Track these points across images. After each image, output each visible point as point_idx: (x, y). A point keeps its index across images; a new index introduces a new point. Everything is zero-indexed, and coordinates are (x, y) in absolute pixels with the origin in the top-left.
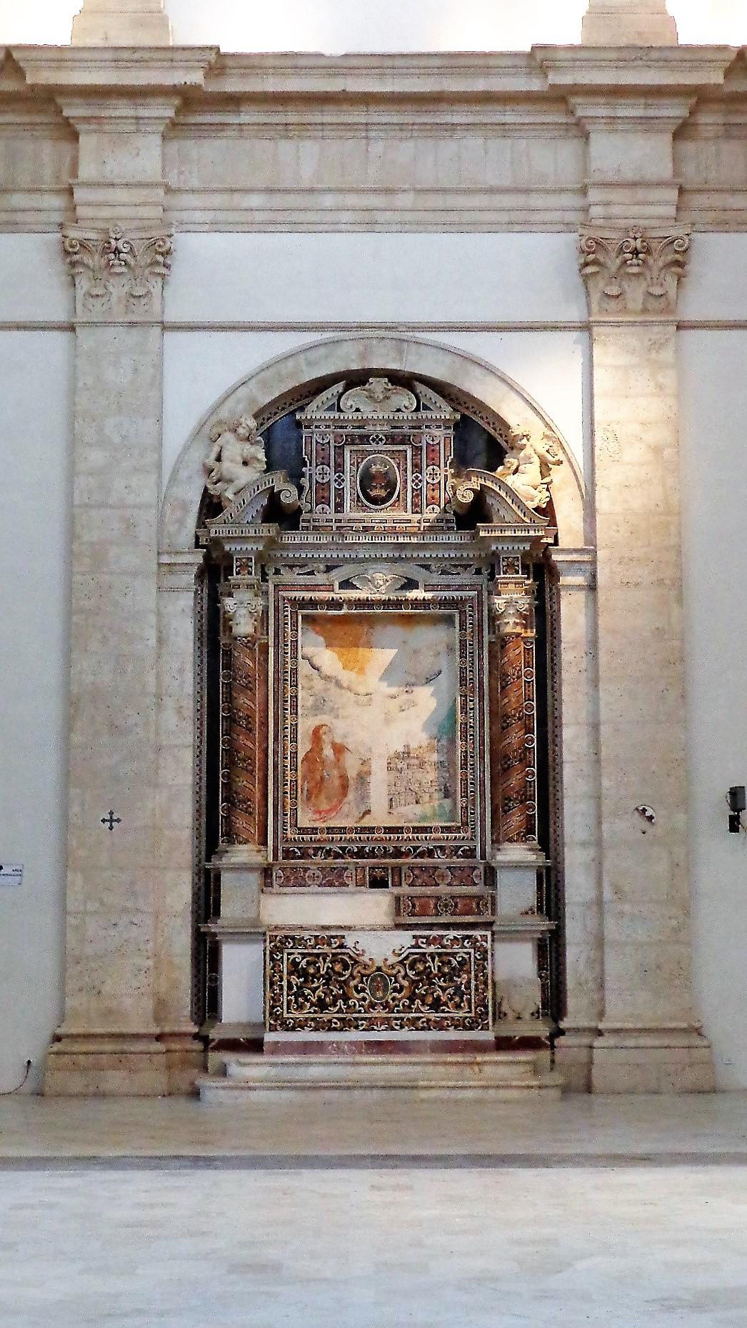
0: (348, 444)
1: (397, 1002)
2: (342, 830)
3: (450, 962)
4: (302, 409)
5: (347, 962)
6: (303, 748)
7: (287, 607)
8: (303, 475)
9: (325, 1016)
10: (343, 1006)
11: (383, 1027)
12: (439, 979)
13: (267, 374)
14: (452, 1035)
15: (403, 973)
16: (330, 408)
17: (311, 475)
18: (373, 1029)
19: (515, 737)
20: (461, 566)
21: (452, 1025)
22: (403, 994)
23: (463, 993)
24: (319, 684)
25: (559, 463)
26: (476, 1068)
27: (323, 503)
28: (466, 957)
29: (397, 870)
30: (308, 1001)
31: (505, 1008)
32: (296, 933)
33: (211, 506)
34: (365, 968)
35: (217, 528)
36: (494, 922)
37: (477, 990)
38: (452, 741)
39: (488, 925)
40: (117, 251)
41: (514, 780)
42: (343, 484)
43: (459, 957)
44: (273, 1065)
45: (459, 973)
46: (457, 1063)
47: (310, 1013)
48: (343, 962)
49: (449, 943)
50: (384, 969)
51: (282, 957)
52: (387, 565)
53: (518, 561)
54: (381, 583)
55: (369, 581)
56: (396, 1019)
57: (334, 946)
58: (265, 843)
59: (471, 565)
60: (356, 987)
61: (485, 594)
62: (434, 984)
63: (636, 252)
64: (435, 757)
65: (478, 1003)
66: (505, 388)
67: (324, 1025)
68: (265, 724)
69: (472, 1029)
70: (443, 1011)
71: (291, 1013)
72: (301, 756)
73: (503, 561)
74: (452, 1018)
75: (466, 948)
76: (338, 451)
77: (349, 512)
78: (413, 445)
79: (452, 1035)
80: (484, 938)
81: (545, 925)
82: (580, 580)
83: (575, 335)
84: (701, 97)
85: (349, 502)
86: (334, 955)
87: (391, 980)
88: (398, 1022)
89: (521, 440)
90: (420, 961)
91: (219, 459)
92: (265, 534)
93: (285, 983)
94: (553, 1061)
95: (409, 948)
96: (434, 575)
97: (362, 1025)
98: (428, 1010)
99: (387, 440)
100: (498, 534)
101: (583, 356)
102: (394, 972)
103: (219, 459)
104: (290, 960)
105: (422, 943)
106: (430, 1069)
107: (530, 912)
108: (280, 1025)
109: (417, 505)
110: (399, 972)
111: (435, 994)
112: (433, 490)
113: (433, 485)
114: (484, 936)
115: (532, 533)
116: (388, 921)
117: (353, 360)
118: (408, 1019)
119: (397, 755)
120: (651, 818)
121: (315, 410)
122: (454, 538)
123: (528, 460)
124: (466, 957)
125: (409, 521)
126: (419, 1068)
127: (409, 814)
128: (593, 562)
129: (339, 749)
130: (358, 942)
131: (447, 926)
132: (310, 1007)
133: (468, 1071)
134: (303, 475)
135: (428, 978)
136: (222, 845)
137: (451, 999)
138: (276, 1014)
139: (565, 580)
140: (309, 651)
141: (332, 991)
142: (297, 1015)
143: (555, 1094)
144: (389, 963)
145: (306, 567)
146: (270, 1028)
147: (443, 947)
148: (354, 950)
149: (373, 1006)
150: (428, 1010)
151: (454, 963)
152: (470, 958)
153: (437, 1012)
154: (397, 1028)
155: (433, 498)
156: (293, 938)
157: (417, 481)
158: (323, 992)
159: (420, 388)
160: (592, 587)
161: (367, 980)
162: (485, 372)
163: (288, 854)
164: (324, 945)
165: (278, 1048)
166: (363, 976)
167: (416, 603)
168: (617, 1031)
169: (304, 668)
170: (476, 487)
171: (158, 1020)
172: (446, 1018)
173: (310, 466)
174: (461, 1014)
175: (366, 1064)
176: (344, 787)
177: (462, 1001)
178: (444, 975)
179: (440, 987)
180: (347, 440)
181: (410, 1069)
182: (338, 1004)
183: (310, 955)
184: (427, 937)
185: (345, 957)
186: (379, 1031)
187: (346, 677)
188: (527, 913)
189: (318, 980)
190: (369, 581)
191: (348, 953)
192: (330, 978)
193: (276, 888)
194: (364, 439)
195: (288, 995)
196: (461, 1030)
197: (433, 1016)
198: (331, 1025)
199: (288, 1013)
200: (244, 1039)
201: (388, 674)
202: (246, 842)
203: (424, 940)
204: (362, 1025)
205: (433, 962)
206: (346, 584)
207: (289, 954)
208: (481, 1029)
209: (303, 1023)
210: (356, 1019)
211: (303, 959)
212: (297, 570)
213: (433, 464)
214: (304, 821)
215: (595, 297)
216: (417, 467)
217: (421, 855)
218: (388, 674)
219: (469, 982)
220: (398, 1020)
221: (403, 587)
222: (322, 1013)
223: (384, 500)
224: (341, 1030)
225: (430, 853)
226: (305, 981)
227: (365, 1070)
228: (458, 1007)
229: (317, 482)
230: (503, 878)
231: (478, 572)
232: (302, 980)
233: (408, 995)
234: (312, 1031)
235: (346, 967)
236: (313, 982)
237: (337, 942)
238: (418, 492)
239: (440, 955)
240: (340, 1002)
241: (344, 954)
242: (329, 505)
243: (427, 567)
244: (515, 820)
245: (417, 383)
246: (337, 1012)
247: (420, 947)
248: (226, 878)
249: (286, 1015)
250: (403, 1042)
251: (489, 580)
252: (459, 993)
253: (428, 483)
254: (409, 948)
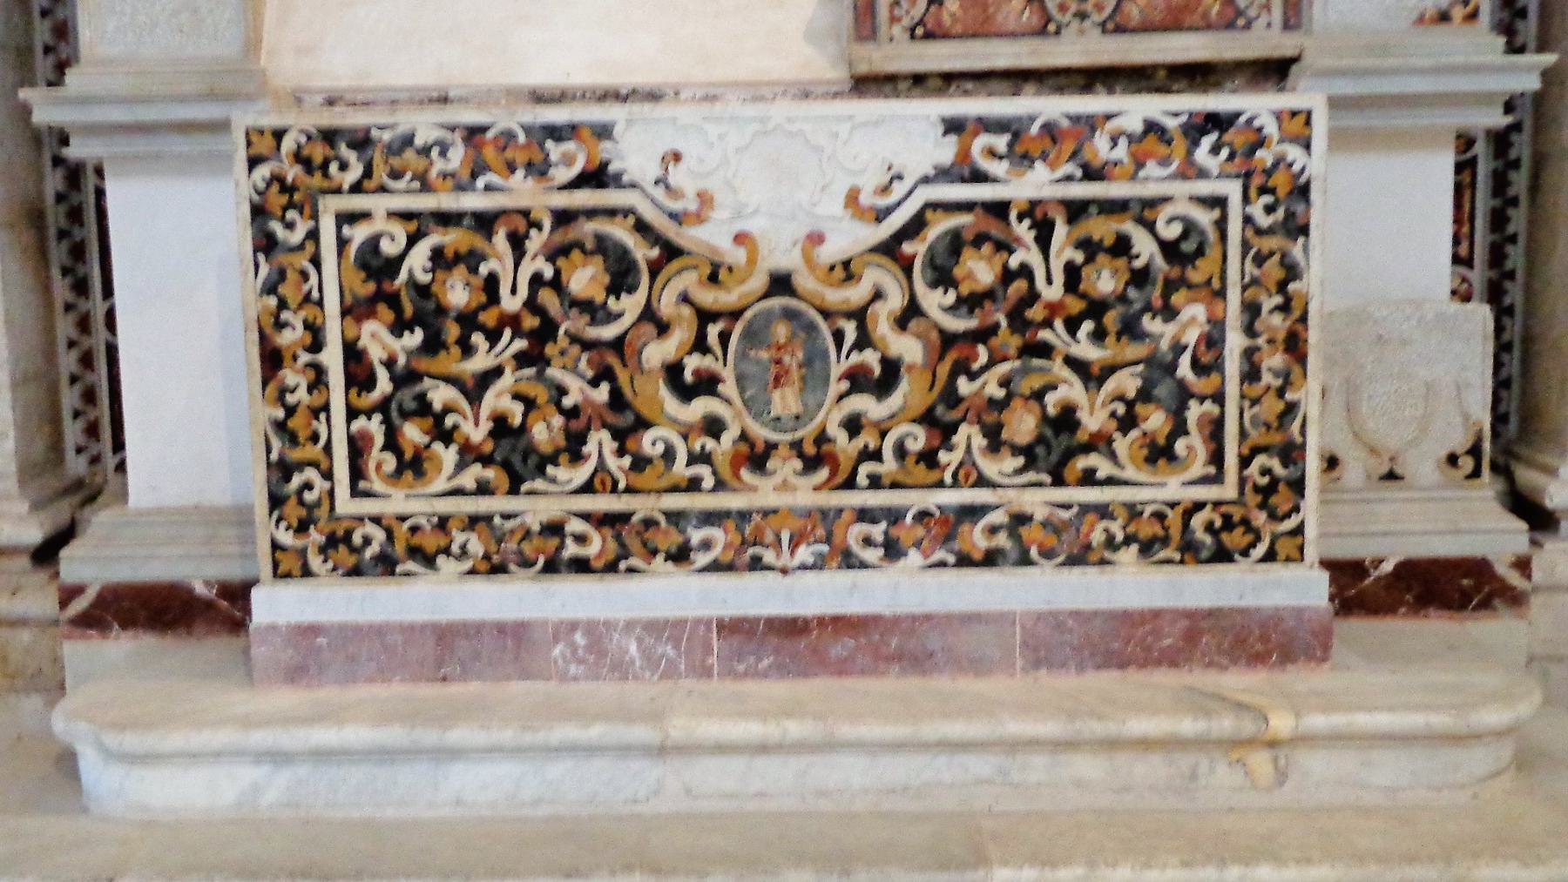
1: (867, 439)
3: (1122, 246)
9: (535, 509)
10: (613, 463)
11: (804, 554)
12: (1072, 326)
15: (895, 301)
18: (756, 564)
21: (1128, 540)
22: (895, 400)
23: (1184, 394)
26: (1260, 762)
28: (1205, 218)
30: (446, 437)
32: (384, 123)
34: (713, 278)
36: (1294, 60)
37: (1251, 374)
43: (1170, 221)
44: (279, 758)
45: (1166, 296)
46: (1170, 744)
47: (458, 492)
49: (1121, 152)
50: (805, 282)
51: (313, 235)
56: (865, 515)
57: (563, 174)
60: (673, 371)
62: (1045, 351)
65: (1256, 436)
67: (527, 548)
69: (1222, 555)
70: (1088, 478)
71: (368, 494)
74: (1134, 512)
75: (1202, 174)
80: (1296, 125)
86: (563, 218)
87: (839, 336)
88: (878, 531)
90: (979, 240)
93: (332, 357)
95: (926, 180)
97: (706, 545)
98: (1020, 471)
102: (856, 294)
104: (352, 250)
105: (992, 153)
106: (1037, 767)
107: (1458, 13)
108: (323, 550)
110: (878, 295)
111: (1051, 399)
114: (1294, 114)
116: (827, 68)
118: (923, 516)
124: (1205, 218)
126: (981, 765)
130: (677, 157)
132: (461, 467)
133: (1221, 776)
135: (1018, 320)
137: (1128, 422)
138: (301, 502)
141: (562, 391)
142: (396, 501)
144: (832, 251)
146: (276, 565)
147: (1092, 174)
148: (659, 193)
149: (757, 457)
150: (1020, 471)
151: (1145, 248)
152: (1221, 225)
153: (1059, 481)
154: (873, 555)
158: (517, 397)
161: (724, 338)
164: (511, 168)
166: (705, 317)
172: (1104, 512)
174: (1172, 487)
175: (722, 749)
177: (1180, 429)
178: (1096, 309)
179: (1073, 363)
181: (942, 768)
182: (590, 448)
183: (446, 219)
184: (1013, 128)
185: (621, 232)
186: (784, 571)
188: (1444, 17)
189: (493, 337)
191: (627, 212)
192: (547, 330)
195: (352, 414)
196: (1169, 561)
197: (1038, 501)
198: (561, 546)
199: (355, 493)
200: (207, 583)
203: (1001, 142)
204: (706, 545)
205: (1044, 242)
207: (347, 218)
208: (1270, 556)
209: (430, 542)
210: (675, 517)
211: (412, 240)
219: (1213, 340)
220: (874, 521)
222: (514, 490)
224: (611, 568)
226: (433, 345)
228: (1160, 453)
232: (415, 338)
233: (919, 406)
234: (472, 572)
235: (621, 277)
236: (467, 350)
237: (568, 159)
239: (1076, 210)
240: (600, 442)
241: (611, 213)
246: (587, 488)
247: (979, 177)
249: (346, 504)
250: (896, 621)
252: (1163, 390)
254: (926, 180)
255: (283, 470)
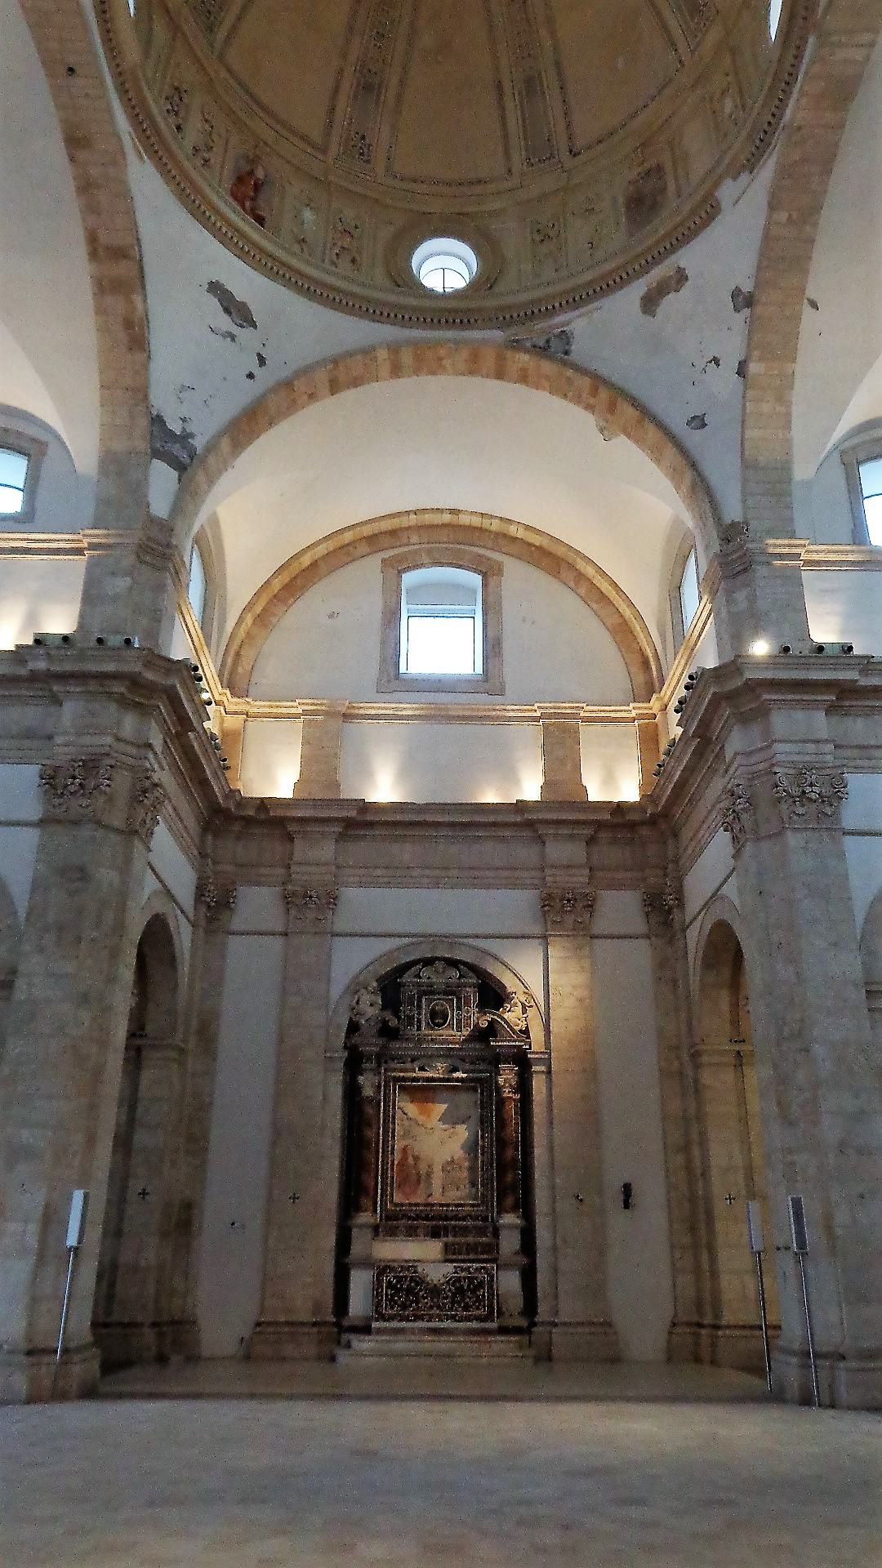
2: (417, 1205)
4: (401, 977)
5: (420, 1281)
6: (397, 1157)
14: (474, 1325)
16: (415, 977)
19: (510, 1153)
24: (406, 1123)
25: (531, 1006)
29: (446, 1228)
31: (504, 1309)
33: (353, 1028)
35: (356, 1039)
38: (476, 1156)
39: (494, 1260)
40: (311, 897)
41: (509, 1177)
48: (415, 1281)
56: (445, 1315)
58: (375, 1211)
63: (569, 901)
64: (467, 1164)
68: (377, 1144)
72: (396, 1162)
77: (424, 1030)
79: (474, 1325)
81: (525, 1261)
82: (543, 1068)
83: (537, 941)
84: (599, 825)
91: (358, 1003)
94: (530, 1341)
100: (500, 1044)
103: (358, 1003)
115: (517, 1043)
116: (439, 1256)
119: (448, 1163)
120: (581, 1200)
121: (407, 978)
123: (515, 1005)
125: (455, 1036)
127: (453, 1196)
128: (550, 1059)
129: (416, 1158)
131: (473, 1261)
136: (353, 1214)
139: (534, 1068)
140: (402, 1104)
143: (530, 1362)
149: (431, 1307)
156: (389, 1267)
160: (549, 1072)
163: (388, 1218)
165: (379, 1331)
167: (457, 1080)
168: (565, 1324)
169: (399, 1114)
171: (314, 1314)
176: (418, 1181)
187: (421, 1119)
193: (381, 1236)
194: (432, 993)
201: (443, 1119)
202: (366, 1211)
206: (422, 1069)
214: (396, 1199)
215: (549, 923)
216: (459, 1008)
217: (459, 1219)
218: (443, 1119)
225: (464, 1219)
227: (426, 1345)
228: (478, 1308)
230: (504, 1234)
237: (412, 1270)
244: (510, 1201)
248: (355, 1232)
255: (377, 1307)
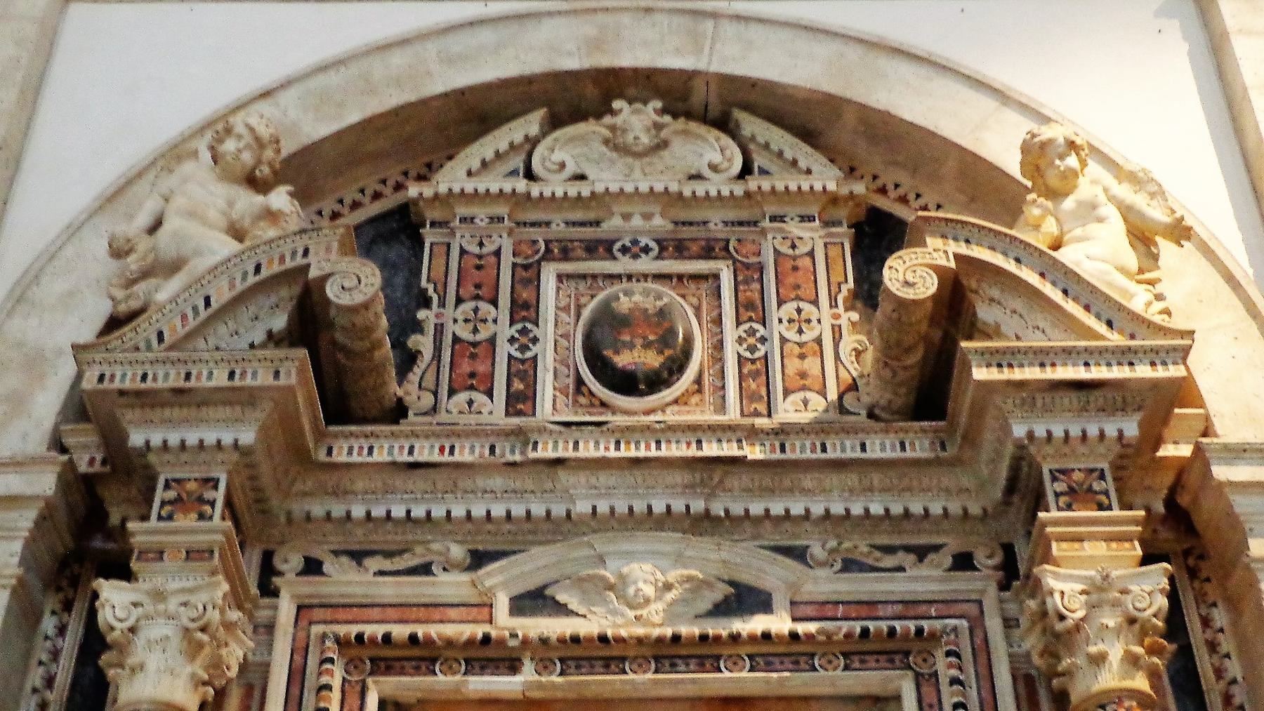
0: (554, 260)
7: (331, 661)
8: (418, 327)
13: (333, 79)
17: (439, 329)
20: (908, 549)
27: (472, 388)
42: (535, 349)
52: (669, 541)
53: (1102, 477)
54: (649, 591)
55: (611, 587)
59: (936, 548)
61: (994, 625)
66: (987, 103)
73: (1054, 479)
76: (521, 273)
78: (735, 261)
85: (549, 392)
89: (1062, 157)
92: (264, 378)
96: (822, 573)
99: (662, 249)
101: (1186, 38)
109: (754, 397)
112: (802, 357)
113: (800, 345)
117: (570, 54)
122: (880, 447)
123: (1089, 211)
134: (418, 327)
145: (406, 556)
155: (803, 375)
157: (754, 341)
159: (751, 125)
162: (924, 71)
170: (942, 262)
173: (442, 304)
180: (548, 250)
190: (611, 587)
194: (601, 247)
212: (374, 564)
213: (798, 298)
216: (753, 311)
221: (722, 609)
223: (656, 382)
229: (456, 340)
231: (963, 562)
238: (759, 365)
242: (490, 394)
243: (798, 554)
245: (740, 116)
251: (1004, 586)
253: (783, 340)
